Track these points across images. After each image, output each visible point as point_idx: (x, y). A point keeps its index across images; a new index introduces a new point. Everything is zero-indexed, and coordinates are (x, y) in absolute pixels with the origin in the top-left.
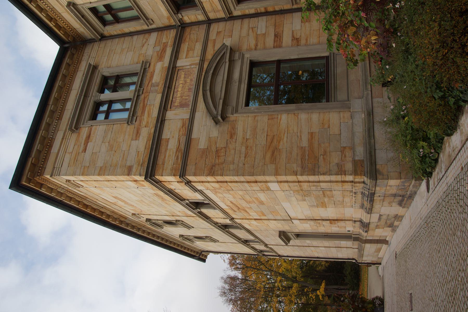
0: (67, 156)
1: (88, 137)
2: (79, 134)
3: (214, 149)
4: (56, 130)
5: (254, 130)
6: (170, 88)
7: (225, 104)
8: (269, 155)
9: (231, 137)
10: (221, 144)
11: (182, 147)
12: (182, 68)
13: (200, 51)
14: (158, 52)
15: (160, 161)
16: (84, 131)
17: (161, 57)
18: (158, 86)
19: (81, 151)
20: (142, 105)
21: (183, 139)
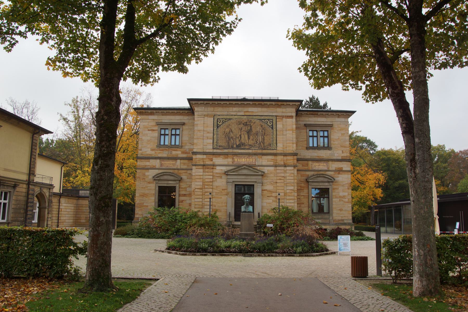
1: (153, 130)
2: (155, 126)
3: (145, 177)
4: (158, 115)
5: (151, 189)
6: (168, 159)
7: (159, 180)
8: (142, 194)
9: (148, 183)
11: (147, 167)
12: (176, 162)
13: (182, 168)
15: (142, 160)
16: (156, 128)
17: (183, 153)
18: (171, 154)
19: (149, 129)
21: (149, 167)
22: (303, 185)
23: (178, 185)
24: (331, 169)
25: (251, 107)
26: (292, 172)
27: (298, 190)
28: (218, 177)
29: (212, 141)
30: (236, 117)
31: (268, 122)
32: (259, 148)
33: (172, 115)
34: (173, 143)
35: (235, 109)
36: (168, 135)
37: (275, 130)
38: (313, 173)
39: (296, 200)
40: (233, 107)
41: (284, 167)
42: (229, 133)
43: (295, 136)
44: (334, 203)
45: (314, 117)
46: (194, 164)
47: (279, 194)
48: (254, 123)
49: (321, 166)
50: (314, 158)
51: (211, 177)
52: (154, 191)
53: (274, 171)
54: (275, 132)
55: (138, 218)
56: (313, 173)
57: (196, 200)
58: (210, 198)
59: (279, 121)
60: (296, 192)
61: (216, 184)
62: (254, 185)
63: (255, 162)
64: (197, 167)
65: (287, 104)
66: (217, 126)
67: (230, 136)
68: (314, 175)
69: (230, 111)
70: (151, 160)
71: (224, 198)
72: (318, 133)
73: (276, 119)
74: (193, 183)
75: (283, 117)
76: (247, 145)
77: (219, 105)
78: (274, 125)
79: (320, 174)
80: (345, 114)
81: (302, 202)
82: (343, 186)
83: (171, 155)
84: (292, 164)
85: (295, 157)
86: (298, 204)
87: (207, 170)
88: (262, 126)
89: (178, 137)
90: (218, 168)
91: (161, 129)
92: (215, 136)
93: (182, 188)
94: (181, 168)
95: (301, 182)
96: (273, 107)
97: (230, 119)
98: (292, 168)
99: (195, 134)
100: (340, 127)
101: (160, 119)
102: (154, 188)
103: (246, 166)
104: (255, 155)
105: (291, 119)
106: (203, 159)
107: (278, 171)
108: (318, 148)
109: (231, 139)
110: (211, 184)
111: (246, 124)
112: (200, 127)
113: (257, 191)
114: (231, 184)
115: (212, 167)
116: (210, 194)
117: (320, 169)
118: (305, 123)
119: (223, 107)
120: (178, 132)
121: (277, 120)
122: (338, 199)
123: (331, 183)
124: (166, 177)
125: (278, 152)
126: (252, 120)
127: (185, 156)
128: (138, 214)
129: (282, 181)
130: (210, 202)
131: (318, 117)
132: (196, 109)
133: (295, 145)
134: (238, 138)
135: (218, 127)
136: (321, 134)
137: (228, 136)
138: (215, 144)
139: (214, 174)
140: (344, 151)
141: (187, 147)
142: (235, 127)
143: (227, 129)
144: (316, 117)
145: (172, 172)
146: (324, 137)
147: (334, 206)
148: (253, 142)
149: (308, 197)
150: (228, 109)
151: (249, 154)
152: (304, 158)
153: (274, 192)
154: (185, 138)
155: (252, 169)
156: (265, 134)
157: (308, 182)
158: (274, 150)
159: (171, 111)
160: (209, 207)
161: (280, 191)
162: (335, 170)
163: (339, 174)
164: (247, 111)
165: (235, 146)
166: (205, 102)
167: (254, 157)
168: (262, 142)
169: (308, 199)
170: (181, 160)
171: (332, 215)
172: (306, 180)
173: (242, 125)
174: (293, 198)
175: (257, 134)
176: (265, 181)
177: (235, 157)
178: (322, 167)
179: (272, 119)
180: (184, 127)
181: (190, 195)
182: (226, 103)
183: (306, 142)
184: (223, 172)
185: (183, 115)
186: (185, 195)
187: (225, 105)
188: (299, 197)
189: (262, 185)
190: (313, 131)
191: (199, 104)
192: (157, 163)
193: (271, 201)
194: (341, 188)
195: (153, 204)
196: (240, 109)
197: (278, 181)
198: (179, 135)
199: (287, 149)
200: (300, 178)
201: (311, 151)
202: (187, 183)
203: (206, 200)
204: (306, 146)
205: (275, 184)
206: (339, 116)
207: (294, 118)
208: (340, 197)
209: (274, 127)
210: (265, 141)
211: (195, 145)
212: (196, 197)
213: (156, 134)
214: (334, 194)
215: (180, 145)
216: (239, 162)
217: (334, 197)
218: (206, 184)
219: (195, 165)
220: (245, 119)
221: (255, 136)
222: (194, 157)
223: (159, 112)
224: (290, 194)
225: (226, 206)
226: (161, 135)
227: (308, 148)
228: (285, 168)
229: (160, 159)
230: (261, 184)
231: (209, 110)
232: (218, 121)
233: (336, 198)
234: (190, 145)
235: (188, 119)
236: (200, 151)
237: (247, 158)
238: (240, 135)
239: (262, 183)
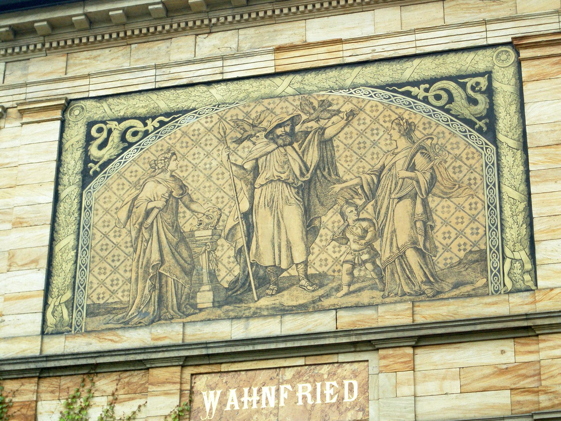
29: (41, 276)
48: (352, 114)
69: (176, 57)
73: (519, 63)
76: (293, 282)
104: (355, 346)
111: (292, 134)
121: (527, 70)
158: (515, 299)
164: (296, 40)
168: (414, 244)
177: (201, 383)
179: (488, 74)
210: (438, 236)
232: (89, 139)
237: (298, 377)
238: (247, 216)
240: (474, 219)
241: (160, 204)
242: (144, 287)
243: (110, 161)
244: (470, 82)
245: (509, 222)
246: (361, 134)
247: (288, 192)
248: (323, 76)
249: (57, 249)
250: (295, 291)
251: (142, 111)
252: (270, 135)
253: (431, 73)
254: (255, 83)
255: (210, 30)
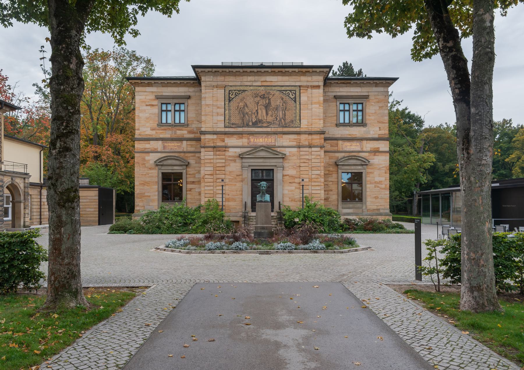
0: (143, 97)
1: (153, 105)
2: (154, 100)
3: (145, 163)
4: (157, 87)
5: (152, 177)
6: (172, 140)
7: (162, 165)
8: (142, 182)
9: (149, 169)
10: (147, 165)
11: (146, 150)
12: (182, 144)
14: (193, 130)
15: (141, 142)
16: (156, 102)
17: (190, 132)
18: (175, 134)
20: (166, 128)
21: (149, 150)
22: (331, 169)
23: (184, 171)
24: (365, 149)
25: (269, 76)
26: (319, 153)
27: (325, 174)
28: (231, 160)
30: (252, 88)
31: (290, 93)
32: (280, 126)
33: (174, 87)
34: (177, 121)
35: (250, 78)
36: (170, 111)
37: (298, 103)
38: (343, 155)
39: (323, 187)
40: (248, 76)
41: (309, 147)
42: (244, 107)
43: (322, 110)
44: (368, 190)
45: (346, 87)
46: (203, 145)
47: (303, 180)
48: (273, 95)
49: (354, 146)
50: (345, 136)
51: (224, 161)
52: (157, 178)
53: (296, 153)
54: (298, 106)
55: (139, 210)
56: (343, 155)
57: (206, 188)
58: (222, 186)
59: (304, 93)
60: (323, 177)
61: (228, 169)
62: (273, 170)
63: (275, 143)
64: (206, 149)
65: (313, 71)
66: (229, 99)
67: (245, 112)
68: (344, 157)
69: (244, 80)
70: (151, 142)
71: (239, 185)
72: (351, 106)
73: (300, 89)
74: (202, 168)
75: (308, 87)
76: (264, 122)
77: (231, 74)
78: (297, 98)
79: (352, 156)
80: (384, 82)
81: (330, 189)
82: (379, 169)
83: (176, 135)
84: (318, 144)
85: (323, 136)
86: (325, 191)
87: (218, 153)
88: (282, 99)
89: (182, 114)
90: (231, 150)
91: (162, 104)
92: (227, 112)
93: (190, 174)
94: (188, 150)
95: (329, 165)
96: (296, 75)
97: (244, 91)
98: (318, 149)
99: (203, 109)
100: (377, 98)
101: (160, 91)
102: (156, 175)
103: (264, 147)
104: (274, 134)
105: (318, 90)
106: (213, 139)
107: (302, 153)
108: (350, 125)
109: (246, 116)
110: (223, 169)
111: (264, 97)
112: (209, 102)
113: (278, 176)
114: (247, 169)
115: (224, 149)
116: (223, 180)
117: (352, 150)
118: (335, 94)
119: (235, 76)
120: (182, 107)
121: (301, 91)
122: (373, 185)
123: (365, 167)
124: (170, 162)
125: (302, 130)
126: (271, 91)
127: (192, 136)
128: (138, 205)
129: (306, 164)
130: (222, 190)
131: (351, 87)
132: (203, 78)
133: (322, 122)
134: (254, 114)
135: (230, 101)
136: (355, 107)
137: (242, 112)
138: (227, 121)
139: (227, 158)
140: (381, 128)
141: (194, 126)
142: (250, 102)
143: (241, 103)
144: (349, 87)
145: (177, 155)
146: (357, 111)
147: (368, 193)
148: (272, 118)
149: (337, 183)
150: (242, 77)
151: (267, 133)
152: (334, 137)
153: (297, 178)
154: (192, 115)
155: (271, 151)
156: (286, 108)
157: (338, 165)
158: (297, 128)
159: (172, 82)
160: (221, 196)
161: (304, 176)
162: (371, 151)
163: (375, 155)
164: (265, 80)
165: (251, 124)
166: (214, 70)
167: (273, 136)
168: (282, 118)
169: (337, 185)
170: (188, 142)
171: (366, 204)
172: (336, 163)
173: (259, 98)
174: (319, 184)
175: (277, 109)
176: (286, 165)
177: (250, 137)
178: (354, 147)
179: (295, 91)
180: (190, 101)
181: (199, 182)
182: (239, 71)
183: (335, 118)
184: (237, 154)
185: (188, 86)
186: (193, 183)
187: (237, 73)
188: (326, 183)
189: (283, 170)
190: (344, 104)
191: (206, 72)
192: (158, 145)
193: (293, 188)
194: (376, 173)
195: (157, 193)
196: (256, 78)
197: (302, 165)
198: (184, 111)
199: (313, 126)
200: (328, 161)
201: (341, 128)
202: (197, 169)
203: (218, 188)
204: (336, 122)
205: (298, 168)
206: (377, 85)
207: (322, 87)
208: (376, 182)
209: (297, 99)
210: (286, 117)
211: (202, 123)
212: (206, 184)
213: (156, 110)
214: (368, 179)
215: (186, 123)
216: (256, 142)
217: (369, 183)
218: (218, 169)
219: (204, 147)
220: (262, 90)
221: (275, 111)
222: (203, 137)
223: (158, 83)
224: (315, 180)
225: (242, 194)
226: (162, 111)
227: (338, 125)
228: (310, 149)
229: (162, 140)
230: (282, 169)
231: (220, 80)
232: (229, 94)
233: (371, 183)
234: (198, 123)
235: (194, 92)
236: (210, 130)
238: (257, 110)
239: (283, 167)
240: (292, 115)
241: (243, 107)
242: (241, 121)
243: (233, 98)
244: (293, 92)
245: (297, 116)
246: (275, 98)
247: (263, 107)
248: (269, 87)
249: (226, 113)
250: (265, 124)
251: (239, 89)
252: (260, 97)
253: (286, 89)
254: (258, 87)
255: (250, 76)
